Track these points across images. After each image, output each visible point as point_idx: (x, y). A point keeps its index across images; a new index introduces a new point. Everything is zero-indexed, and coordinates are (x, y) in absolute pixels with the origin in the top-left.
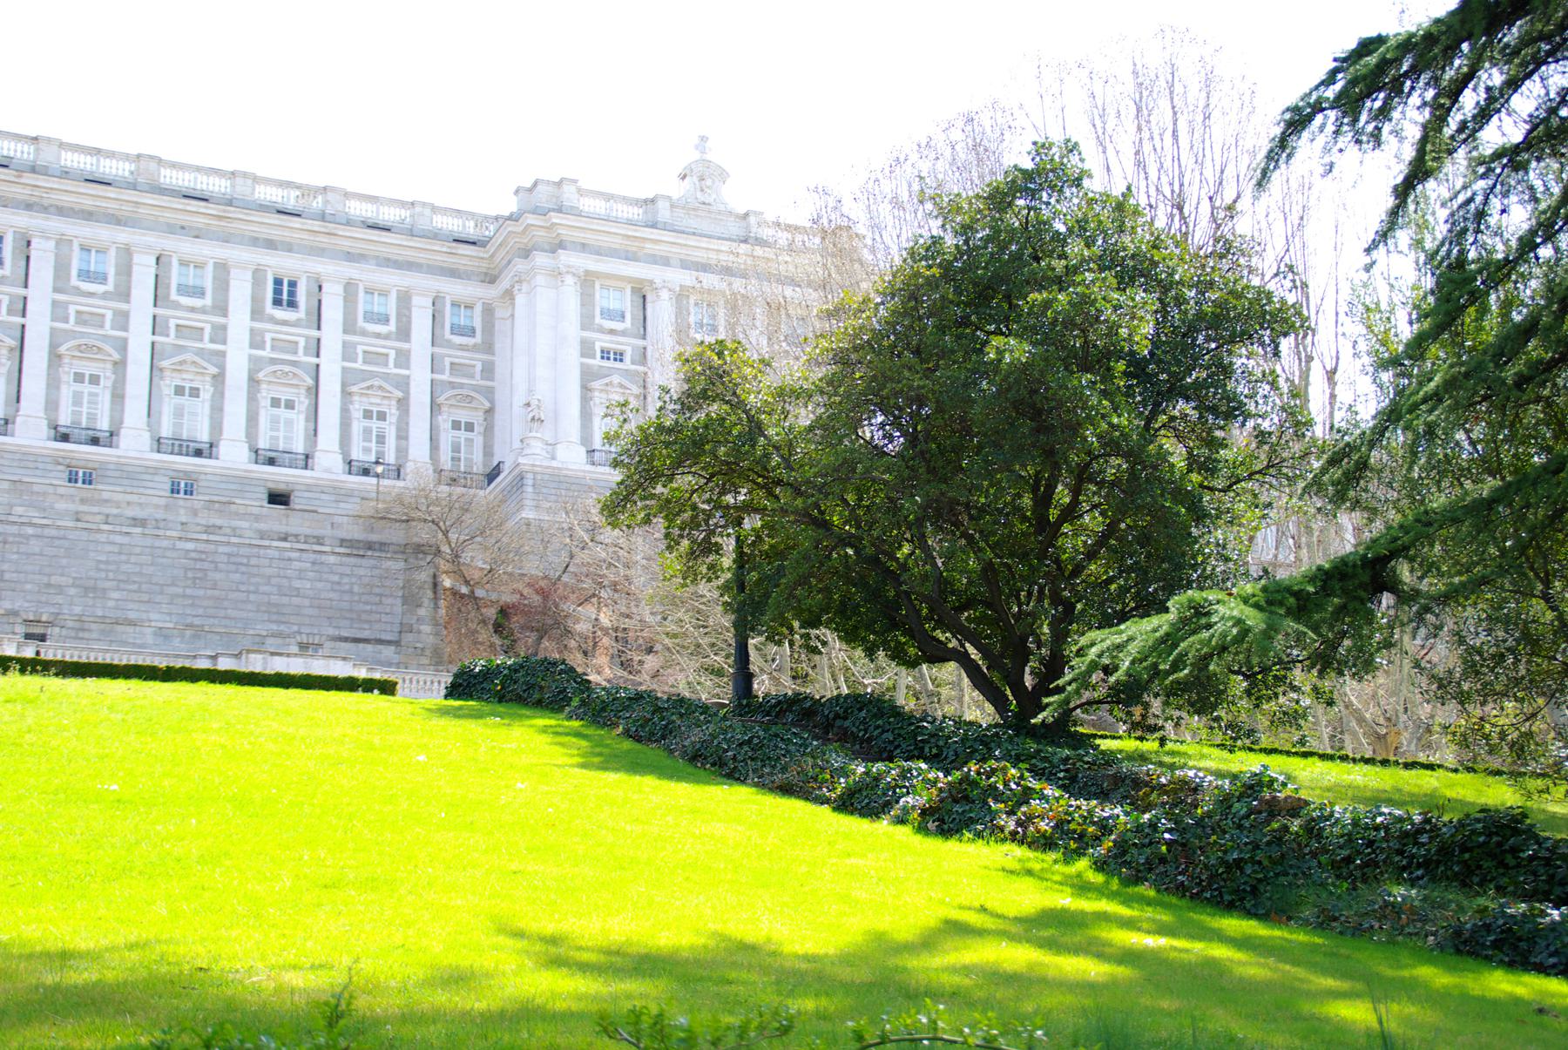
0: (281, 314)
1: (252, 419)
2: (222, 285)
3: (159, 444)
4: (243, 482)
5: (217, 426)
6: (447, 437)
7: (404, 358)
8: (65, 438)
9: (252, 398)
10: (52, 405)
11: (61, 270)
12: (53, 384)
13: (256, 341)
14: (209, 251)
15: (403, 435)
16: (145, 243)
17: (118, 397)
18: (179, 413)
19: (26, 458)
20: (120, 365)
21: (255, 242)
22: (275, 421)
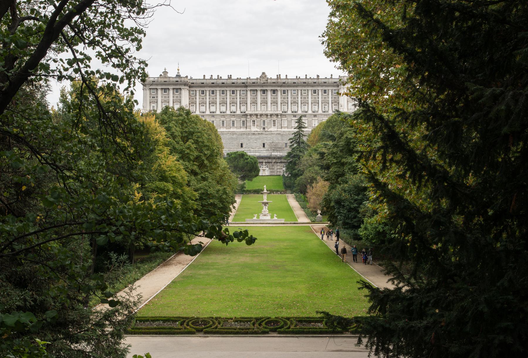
0: (314, 95)
1: (312, 107)
2: (308, 92)
3: (302, 112)
4: (311, 114)
5: (308, 109)
6: (334, 107)
7: (328, 97)
8: (293, 112)
9: (312, 105)
10: (291, 109)
11: (291, 93)
12: (291, 106)
13: (312, 98)
14: (306, 88)
15: (328, 107)
16: (299, 88)
17: (298, 107)
18: (304, 108)
19: (289, 114)
20: (298, 103)
21: (311, 86)
22: (314, 108)
